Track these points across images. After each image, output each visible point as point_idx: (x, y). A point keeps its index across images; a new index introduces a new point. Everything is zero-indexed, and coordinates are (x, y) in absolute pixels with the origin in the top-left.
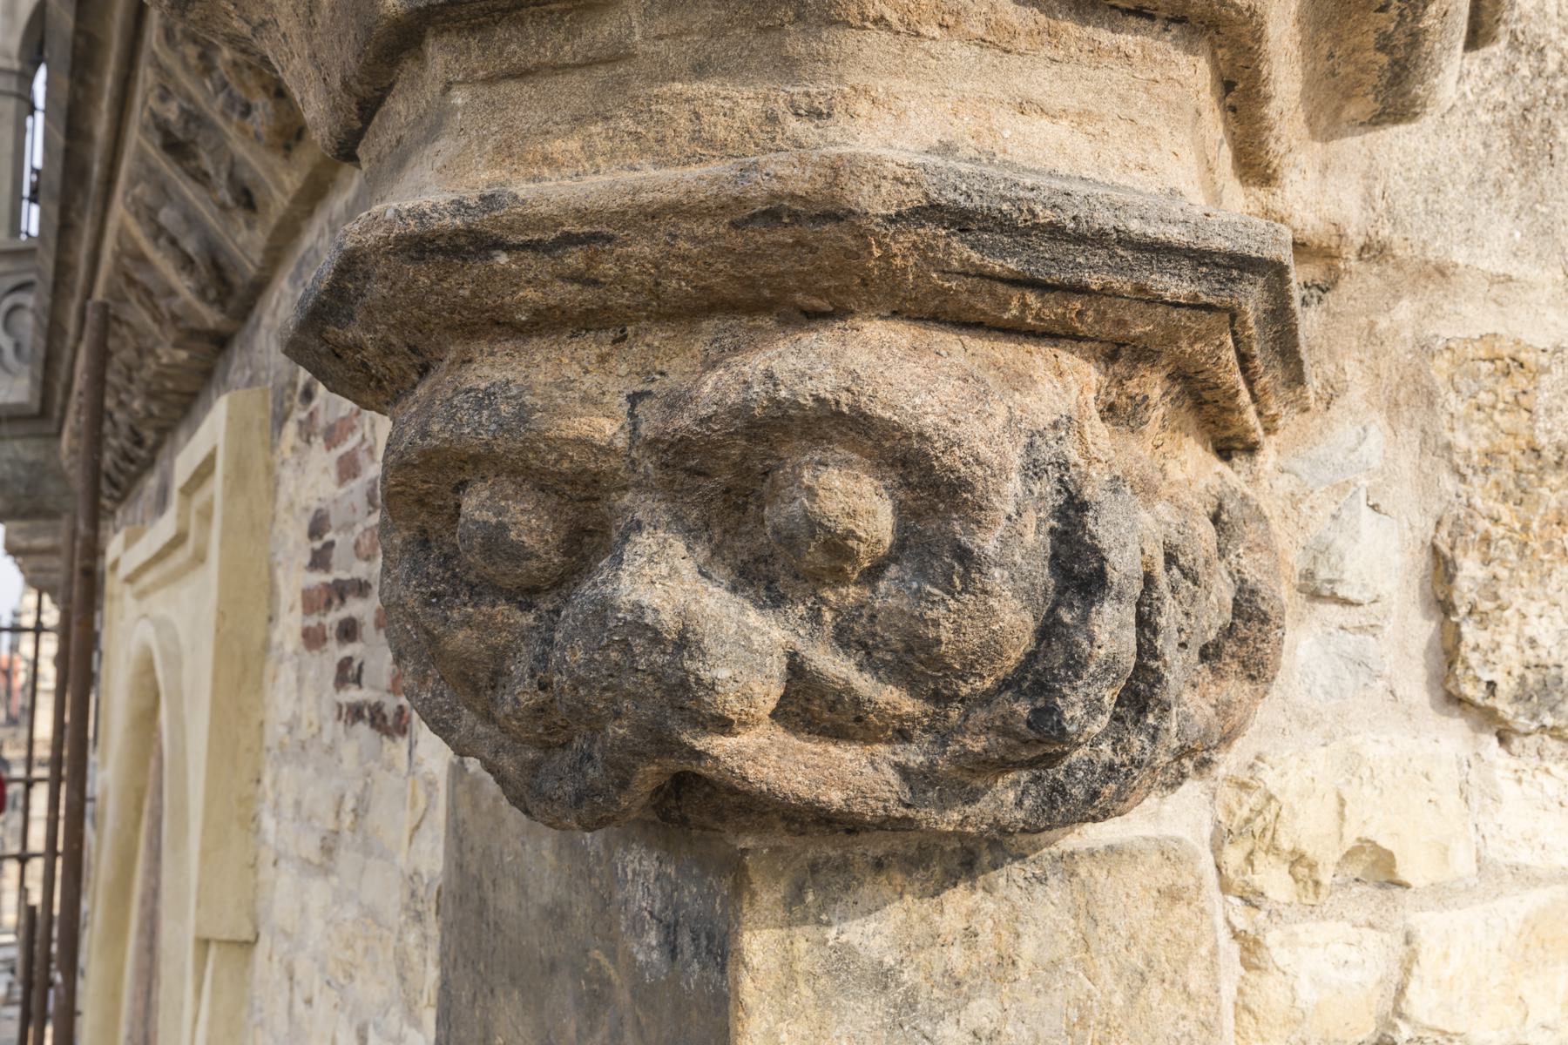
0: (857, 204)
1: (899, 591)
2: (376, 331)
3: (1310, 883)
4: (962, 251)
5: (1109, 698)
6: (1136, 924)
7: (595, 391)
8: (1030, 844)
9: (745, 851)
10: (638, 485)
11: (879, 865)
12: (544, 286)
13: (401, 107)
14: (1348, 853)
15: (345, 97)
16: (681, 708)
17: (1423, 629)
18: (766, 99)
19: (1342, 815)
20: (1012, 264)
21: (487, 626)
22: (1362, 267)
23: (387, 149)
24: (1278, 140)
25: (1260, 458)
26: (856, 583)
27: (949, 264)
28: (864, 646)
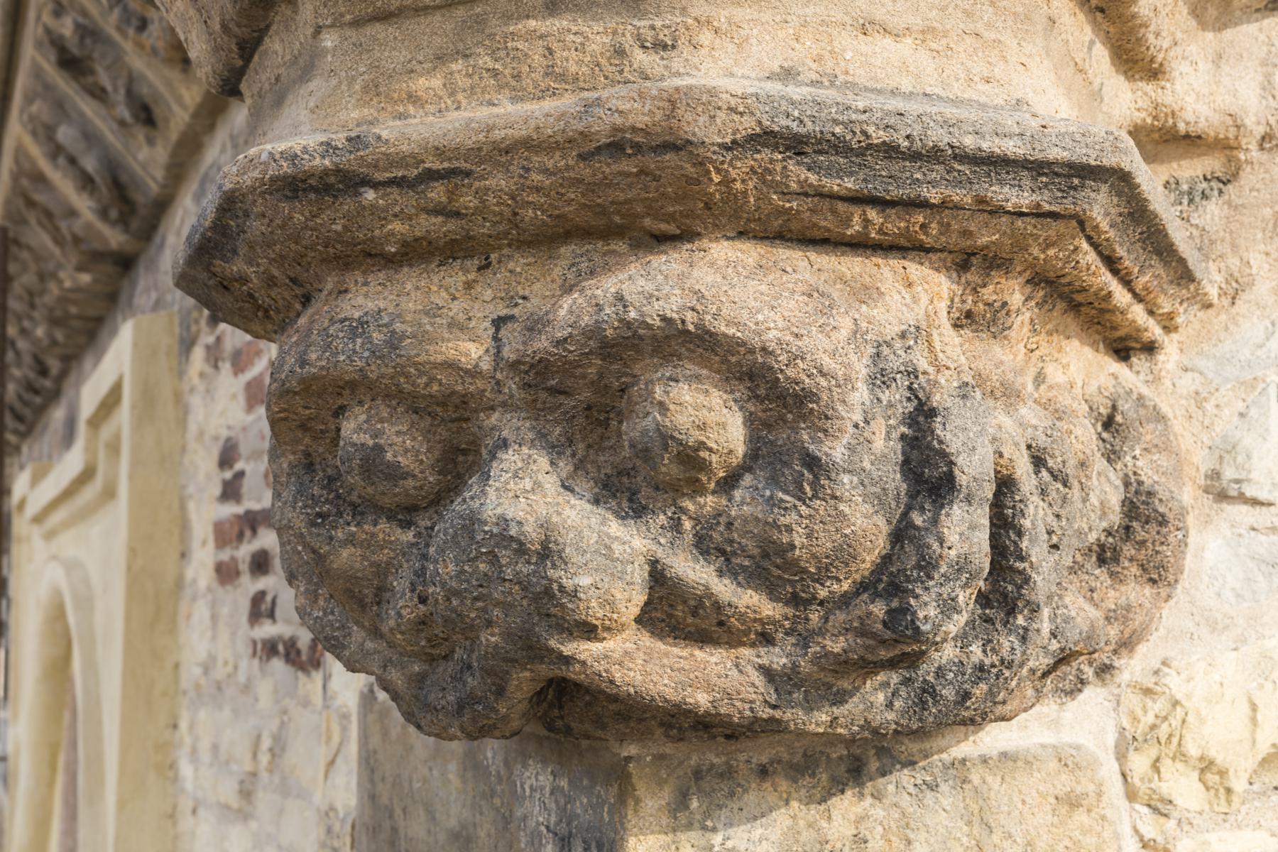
0: (694, 134)
1: (753, 498)
2: (258, 265)
3: (1222, 791)
4: (798, 173)
5: (965, 597)
6: (1032, 831)
7: (461, 317)
8: (921, 751)
9: (628, 759)
10: (504, 404)
11: (763, 772)
12: (410, 219)
13: (277, 46)
14: (1264, 759)
15: (226, 38)
16: (548, 615)
18: (615, 33)
19: (1254, 721)
20: (849, 183)
21: (369, 544)
22: (1264, 157)
23: (267, 86)
24: (1157, 35)
25: (1161, 357)
26: (714, 492)
27: (787, 186)
28: (723, 552)
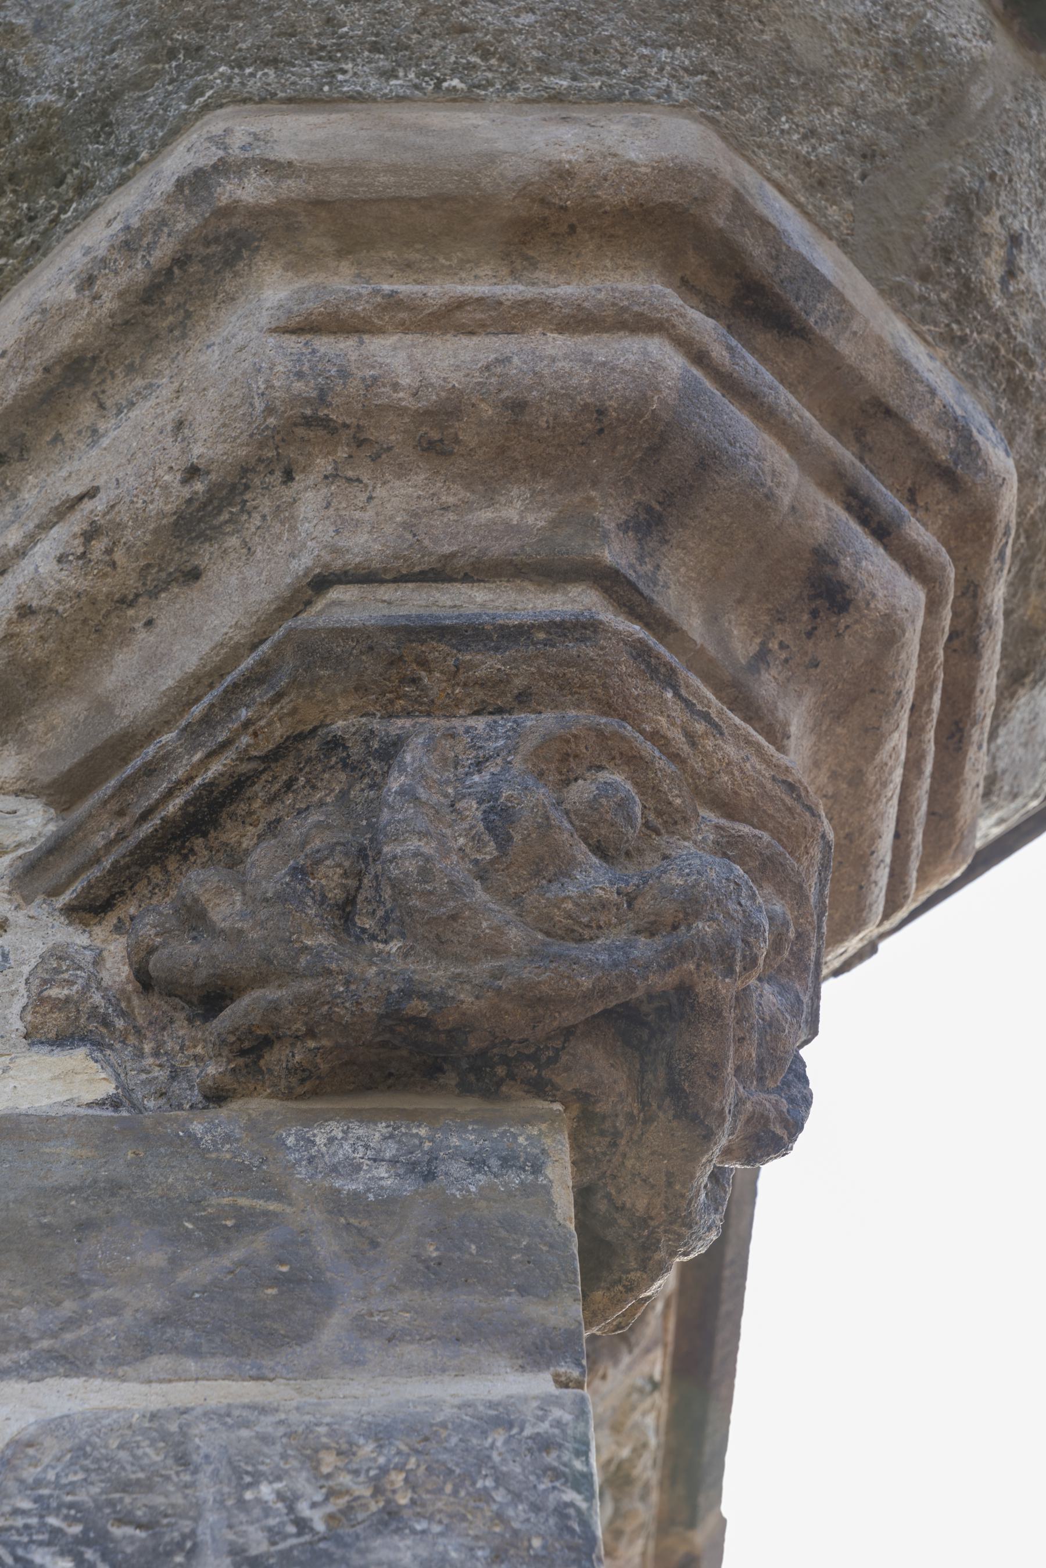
12: (673, 725)
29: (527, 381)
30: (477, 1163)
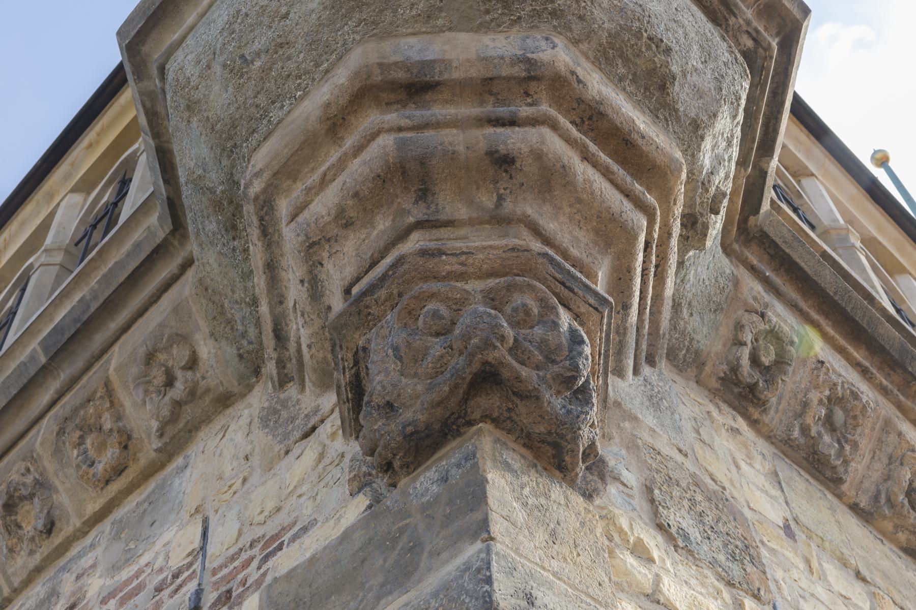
4: (551, 269)
17: (646, 506)
29: (353, 184)
30: (458, 466)
